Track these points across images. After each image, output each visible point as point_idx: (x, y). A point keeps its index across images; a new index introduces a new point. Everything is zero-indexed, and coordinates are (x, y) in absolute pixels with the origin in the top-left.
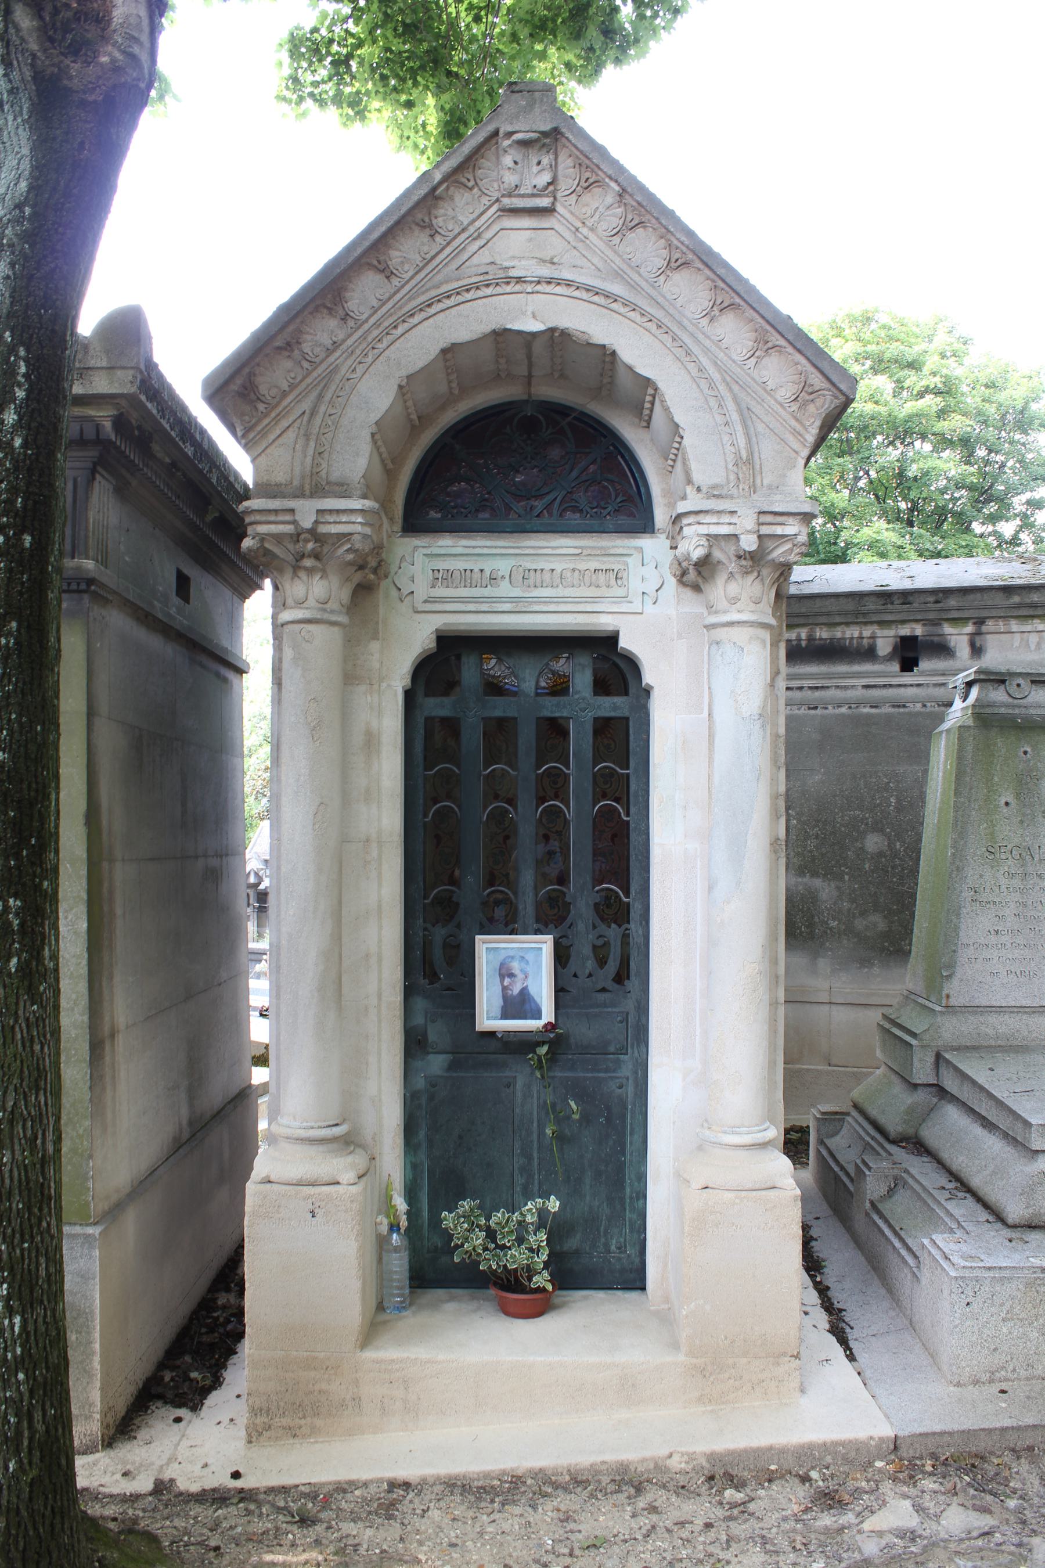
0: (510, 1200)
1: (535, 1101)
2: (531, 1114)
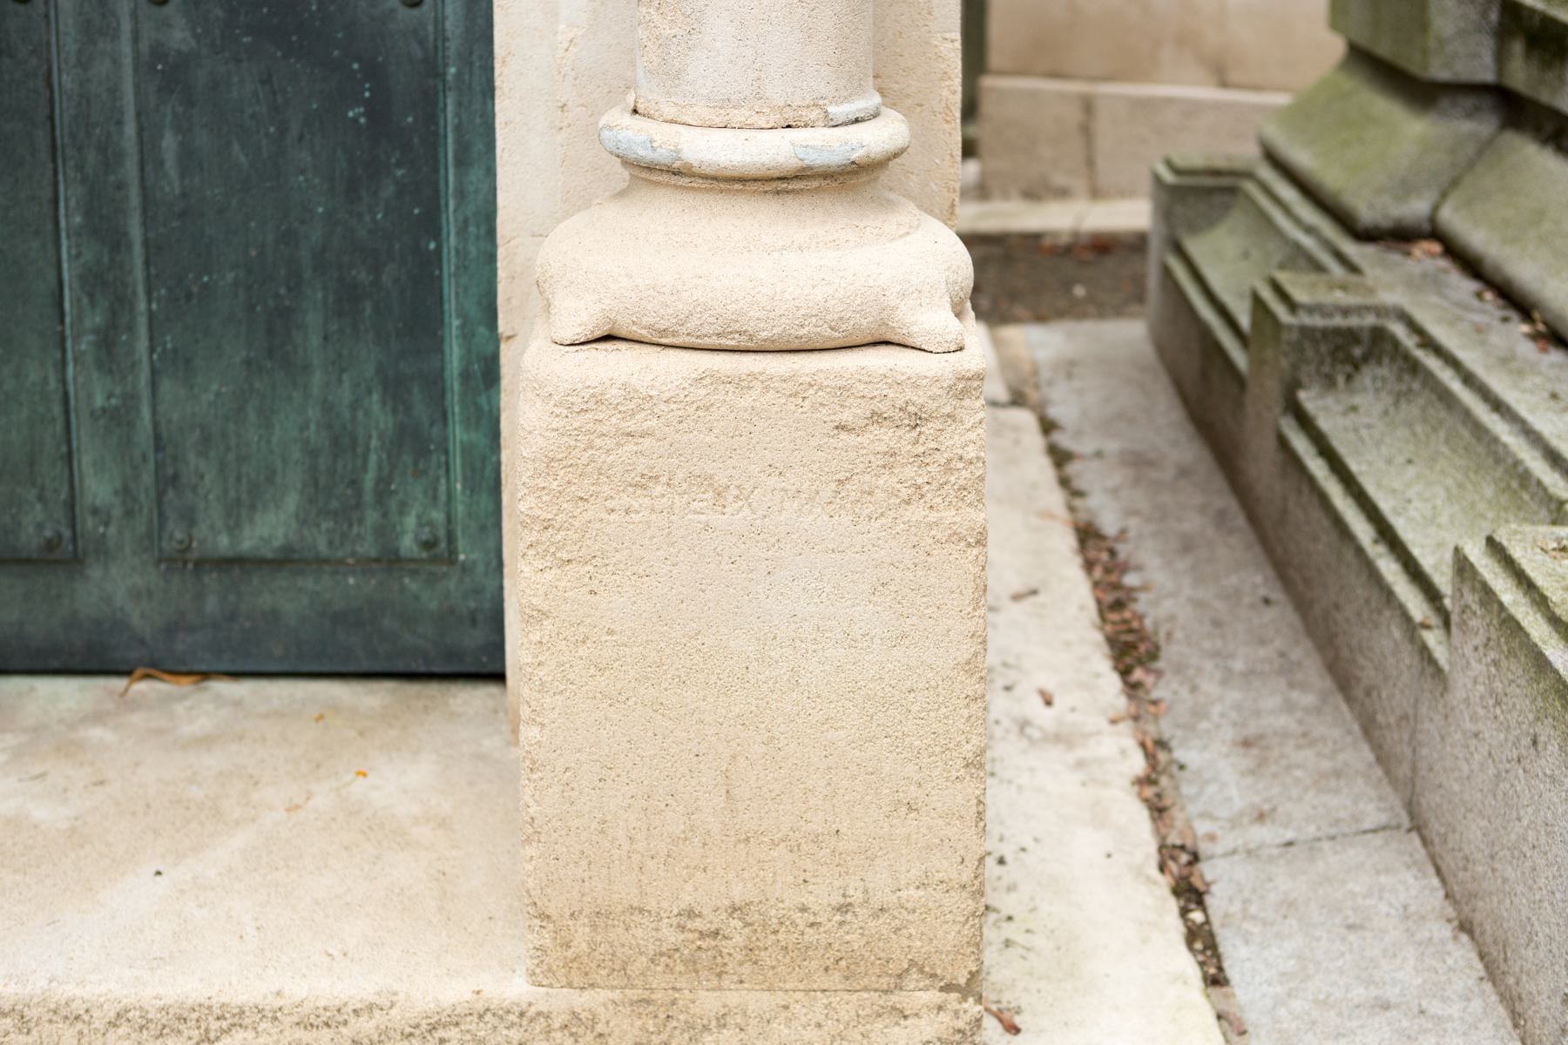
0: (53, 384)
1: (126, 47)
2: (114, 91)
